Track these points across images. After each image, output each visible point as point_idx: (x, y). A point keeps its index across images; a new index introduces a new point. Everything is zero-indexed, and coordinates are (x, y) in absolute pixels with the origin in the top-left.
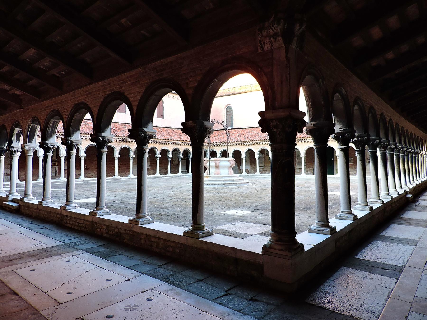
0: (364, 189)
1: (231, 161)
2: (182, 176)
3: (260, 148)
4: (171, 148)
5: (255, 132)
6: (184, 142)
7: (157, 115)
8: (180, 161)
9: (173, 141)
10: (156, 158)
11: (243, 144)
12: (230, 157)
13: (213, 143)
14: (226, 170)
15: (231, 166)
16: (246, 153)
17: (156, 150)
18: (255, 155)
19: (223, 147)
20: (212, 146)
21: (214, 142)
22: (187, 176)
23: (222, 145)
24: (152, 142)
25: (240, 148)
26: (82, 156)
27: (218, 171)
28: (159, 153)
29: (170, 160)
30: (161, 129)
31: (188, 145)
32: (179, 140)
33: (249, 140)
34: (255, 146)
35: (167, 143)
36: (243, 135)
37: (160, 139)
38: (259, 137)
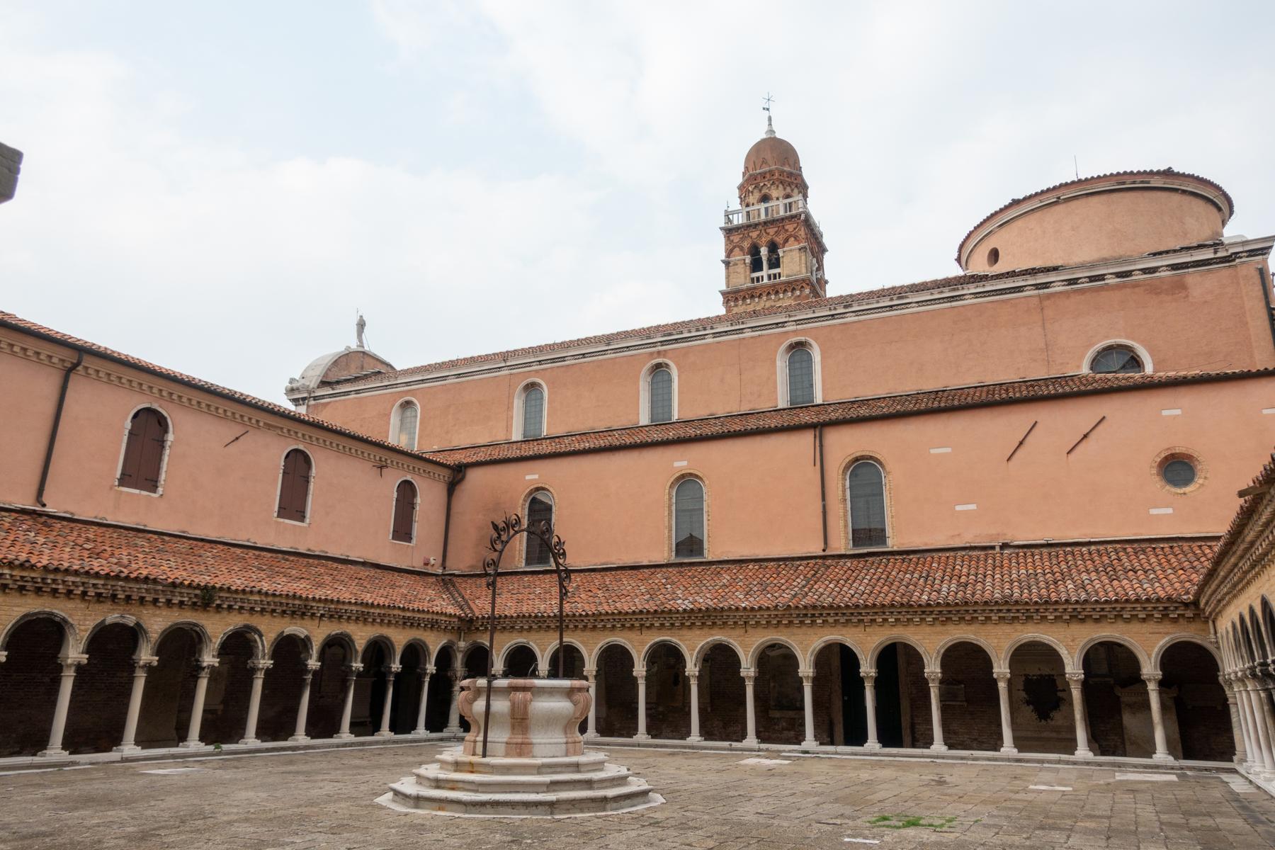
2: (352, 744)
4: (317, 633)
6: (372, 611)
7: (280, 508)
8: (351, 684)
9: (333, 606)
10: (254, 670)
11: (590, 626)
13: (480, 616)
17: (256, 636)
18: (633, 666)
19: (514, 634)
21: (533, 615)
22: (371, 743)
24: (241, 608)
25: (581, 639)
27: (520, 741)
28: (266, 651)
29: (309, 681)
30: (287, 560)
31: (386, 621)
32: (353, 601)
33: (616, 611)
34: (634, 635)
35: (304, 614)
36: (590, 594)
37: (277, 593)
38: (648, 601)
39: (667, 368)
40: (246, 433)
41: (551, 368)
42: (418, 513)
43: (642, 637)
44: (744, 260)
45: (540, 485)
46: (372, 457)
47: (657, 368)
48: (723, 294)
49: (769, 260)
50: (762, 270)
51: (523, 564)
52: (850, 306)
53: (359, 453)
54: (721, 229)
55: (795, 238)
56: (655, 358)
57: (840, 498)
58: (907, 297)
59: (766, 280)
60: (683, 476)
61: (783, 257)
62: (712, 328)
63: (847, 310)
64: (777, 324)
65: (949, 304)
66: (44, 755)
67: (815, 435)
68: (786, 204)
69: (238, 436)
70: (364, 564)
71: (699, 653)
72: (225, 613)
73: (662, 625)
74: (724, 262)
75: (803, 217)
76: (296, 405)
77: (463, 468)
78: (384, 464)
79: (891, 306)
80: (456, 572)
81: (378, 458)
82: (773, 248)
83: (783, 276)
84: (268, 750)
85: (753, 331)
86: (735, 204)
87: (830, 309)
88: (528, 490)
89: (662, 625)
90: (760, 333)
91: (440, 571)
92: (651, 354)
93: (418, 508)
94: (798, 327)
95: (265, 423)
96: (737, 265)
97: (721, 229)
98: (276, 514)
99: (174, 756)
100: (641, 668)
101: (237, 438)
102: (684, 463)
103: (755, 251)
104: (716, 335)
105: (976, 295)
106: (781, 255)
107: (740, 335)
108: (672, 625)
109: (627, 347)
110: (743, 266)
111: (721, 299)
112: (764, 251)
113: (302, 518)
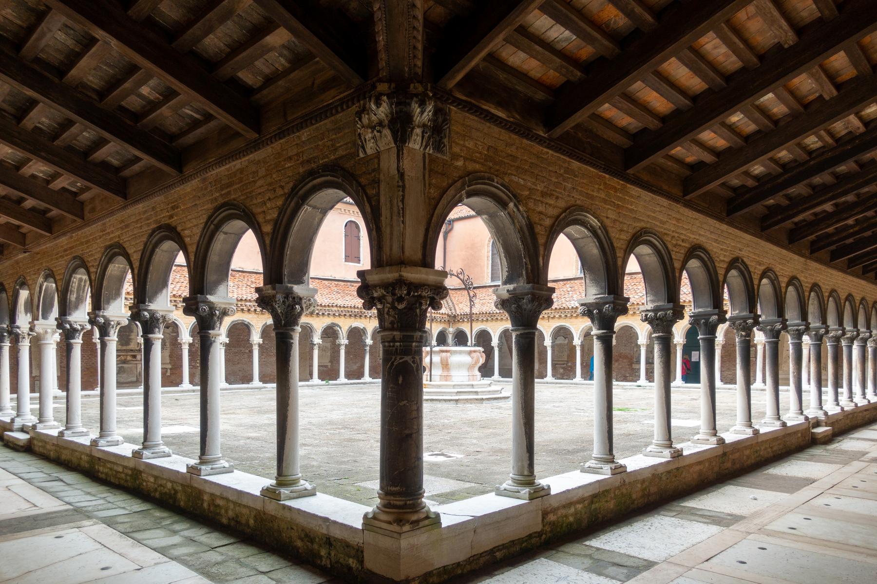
0: (748, 411)
1: (474, 355)
3: (555, 326)
10: (339, 345)
12: (469, 343)
14: (465, 373)
15: (474, 363)
16: (500, 338)
17: (338, 328)
20: (459, 321)
23: (477, 320)
24: (329, 314)
26: (184, 341)
29: (368, 350)
35: (361, 316)
37: (346, 306)
43: (549, 323)
66: (252, 384)
71: (581, 331)
72: (321, 317)
73: (560, 316)
84: (351, 384)
89: (560, 316)
99: (308, 386)
100: (549, 341)
108: (566, 316)
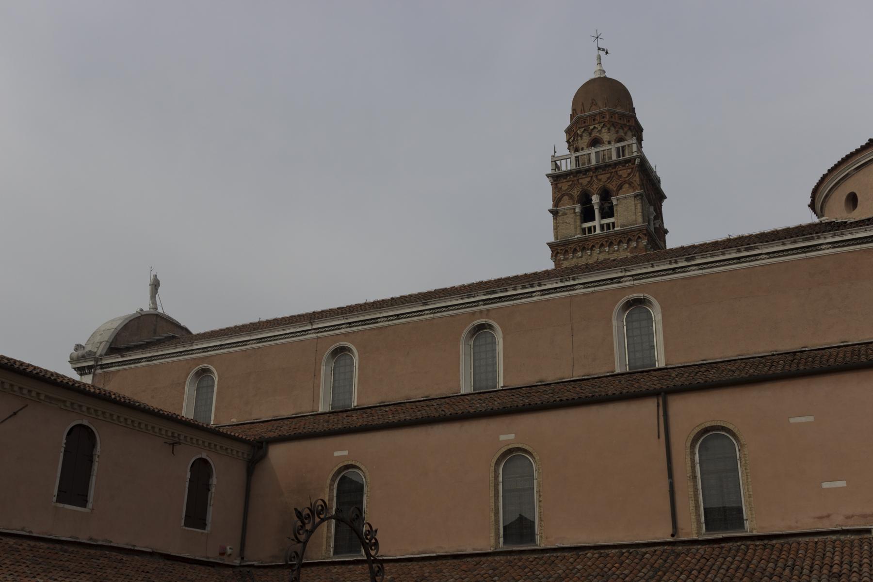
5: (453, 574)
7: (59, 491)
30: (66, 551)
39: (489, 328)
40: (23, 408)
41: (363, 331)
42: (213, 495)
44: (574, 209)
45: (350, 463)
46: (163, 432)
47: (479, 330)
48: (550, 245)
49: (601, 210)
50: (594, 219)
51: (332, 553)
52: (693, 258)
53: (150, 428)
54: (548, 176)
55: (630, 184)
56: (477, 319)
57: (688, 475)
58: (756, 248)
59: (598, 231)
60: (510, 451)
61: (617, 205)
62: (540, 285)
63: (689, 264)
64: (612, 279)
65: (804, 255)
67: (658, 403)
68: (618, 149)
69: (15, 411)
70: (152, 554)
74: (551, 211)
75: (637, 161)
76: (81, 375)
77: (264, 443)
78: (177, 440)
79: (739, 258)
80: (256, 563)
81: (170, 434)
82: (606, 195)
83: (618, 227)
85: (585, 288)
86: (563, 149)
87: (671, 263)
88: (337, 468)
90: (593, 289)
91: (237, 562)
92: (474, 313)
93: (213, 490)
94: (636, 282)
95: (46, 396)
96: (566, 214)
97: (548, 176)
98: (55, 499)
101: (15, 414)
102: (512, 437)
103: (585, 199)
104: (544, 292)
105: (834, 245)
106: (615, 202)
107: (571, 293)
109: (446, 307)
110: (573, 215)
111: (548, 252)
112: (595, 199)
113: (84, 503)
